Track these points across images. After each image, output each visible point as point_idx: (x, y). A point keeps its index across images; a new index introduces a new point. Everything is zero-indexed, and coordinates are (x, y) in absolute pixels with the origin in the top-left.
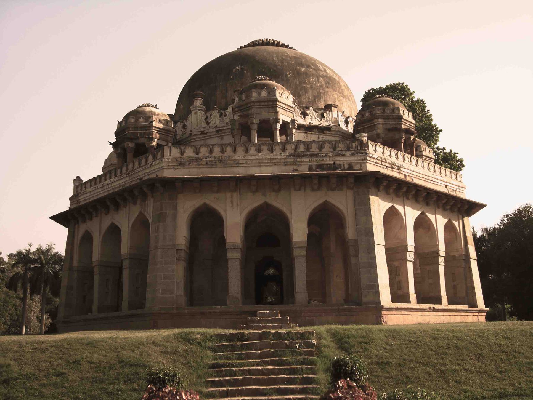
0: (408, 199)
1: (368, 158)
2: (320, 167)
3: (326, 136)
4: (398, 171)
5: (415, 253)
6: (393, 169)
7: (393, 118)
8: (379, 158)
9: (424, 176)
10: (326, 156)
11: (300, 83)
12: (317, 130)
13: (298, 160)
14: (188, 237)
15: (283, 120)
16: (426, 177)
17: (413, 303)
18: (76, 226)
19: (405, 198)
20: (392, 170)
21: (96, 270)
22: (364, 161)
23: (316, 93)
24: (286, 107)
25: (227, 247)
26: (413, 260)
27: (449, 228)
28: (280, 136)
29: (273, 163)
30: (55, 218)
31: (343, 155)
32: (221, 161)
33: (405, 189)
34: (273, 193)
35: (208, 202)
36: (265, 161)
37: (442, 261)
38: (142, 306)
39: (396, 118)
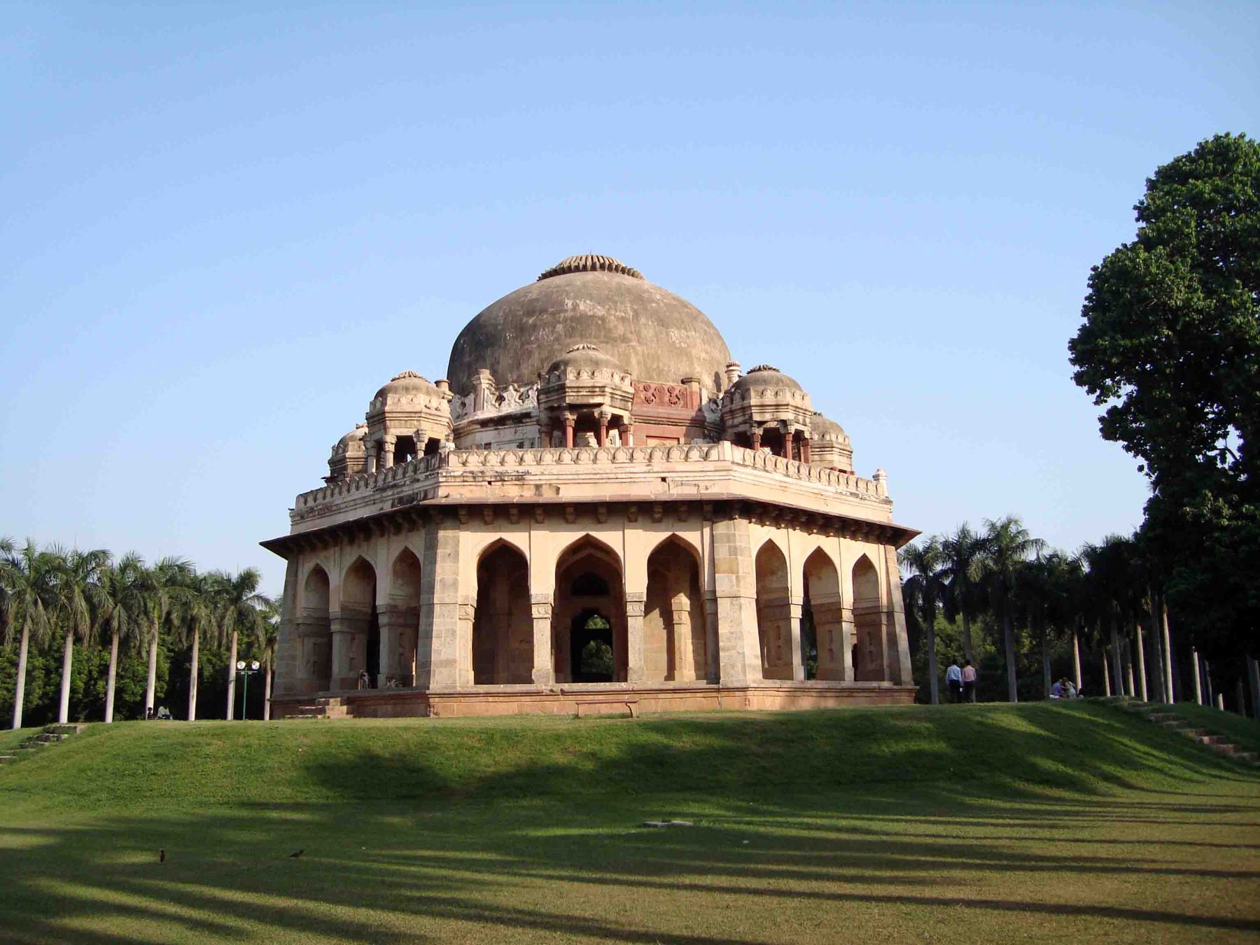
1: (441, 479)
2: (401, 500)
3: (528, 427)
4: (517, 483)
6: (505, 483)
7: (553, 391)
8: (465, 474)
9: (592, 476)
10: (404, 485)
11: (522, 345)
12: (511, 422)
13: (384, 494)
15: (397, 437)
16: (598, 476)
20: (503, 485)
22: (437, 485)
23: (545, 354)
24: (406, 415)
29: (366, 502)
31: (418, 480)
32: (328, 509)
34: (365, 543)
35: (319, 562)
36: (359, 502)
39: (558, 390)
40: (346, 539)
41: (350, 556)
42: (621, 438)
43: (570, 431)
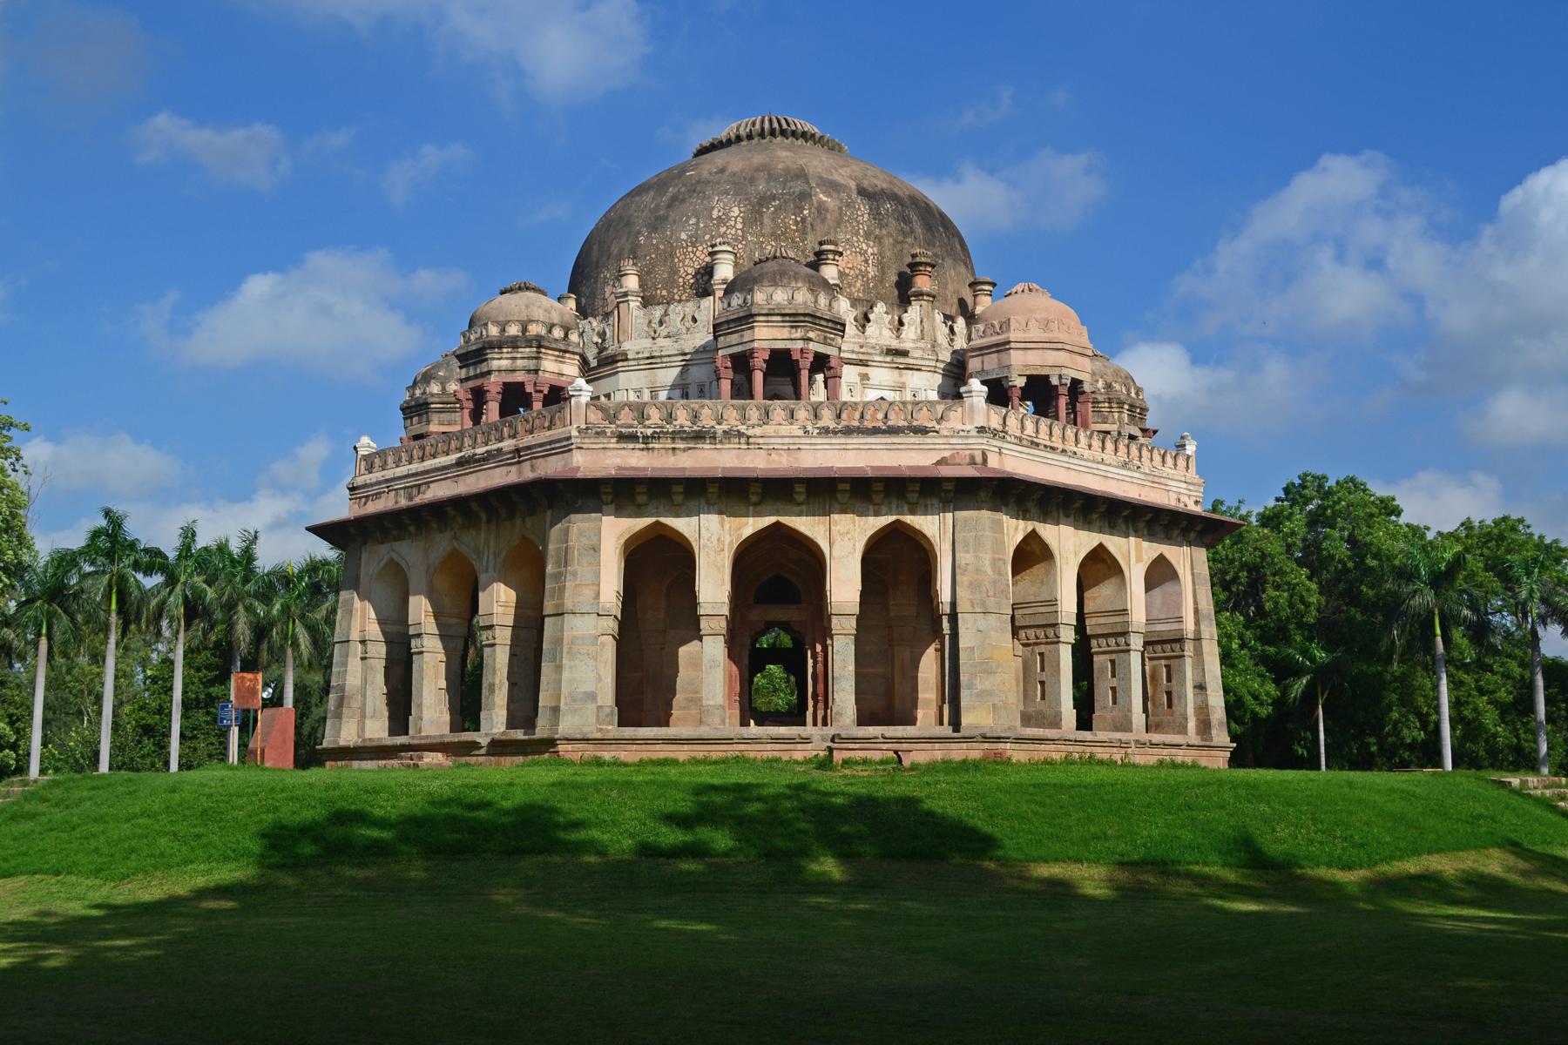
40: (434, 525)
41: (442, 544)
42: (826, 387)
43: (758, 377)
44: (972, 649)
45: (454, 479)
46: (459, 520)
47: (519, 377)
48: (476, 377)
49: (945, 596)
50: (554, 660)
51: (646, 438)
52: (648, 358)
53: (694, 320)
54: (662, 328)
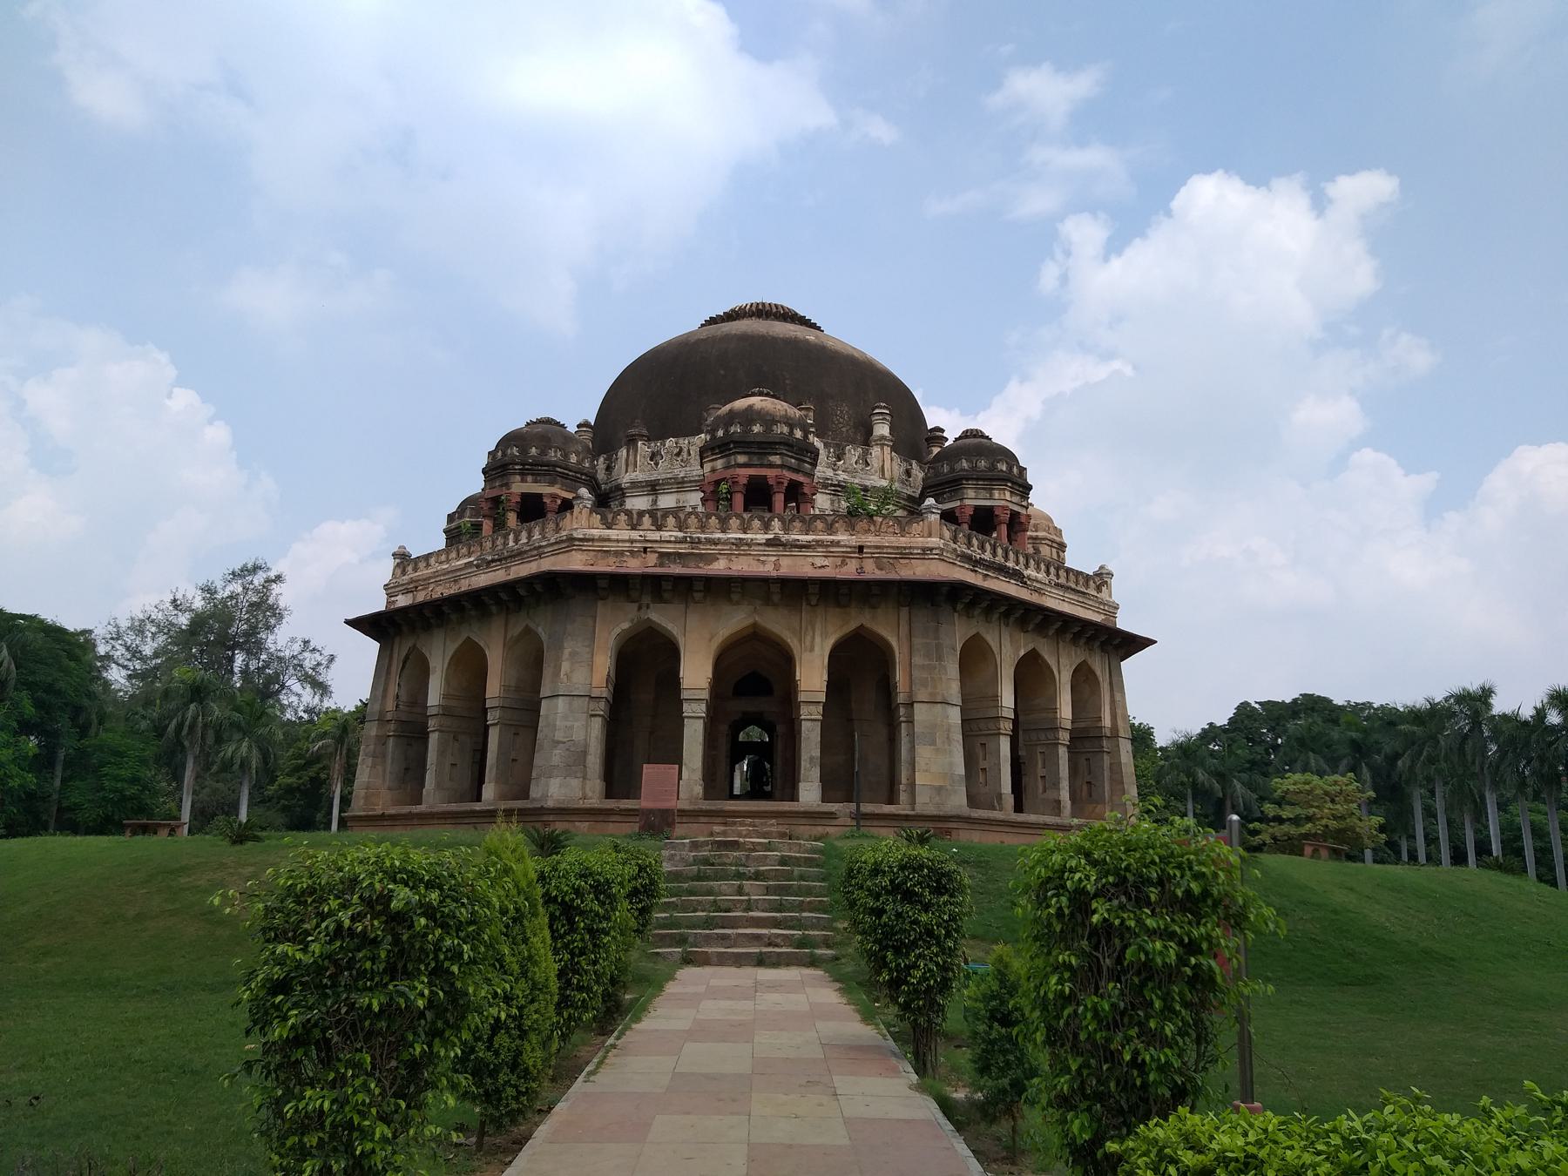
0: (1007, 625)
5: (1015, 722)
14: (613, 674)
17: (1007, 812)
18: (397, 640)
19: (1002, 624)
21: (432, 724)
25: (684, 695)
26: (1011, 733)
27: (1083, 680)
28: (787, 501)
30: (362, 624)
33: (1002, 609)
37: (1064, 737)
38: (524, 794)
44: (1126, 764)
45: (762, 558)
46: (776, 598)
47: (801, 478)
48: (762, 466)
49: (1107, 722)
50: (933, 743)
51: (976, 561)
52: (835, 485)
53: (867, 464)
54: (842, 462)
